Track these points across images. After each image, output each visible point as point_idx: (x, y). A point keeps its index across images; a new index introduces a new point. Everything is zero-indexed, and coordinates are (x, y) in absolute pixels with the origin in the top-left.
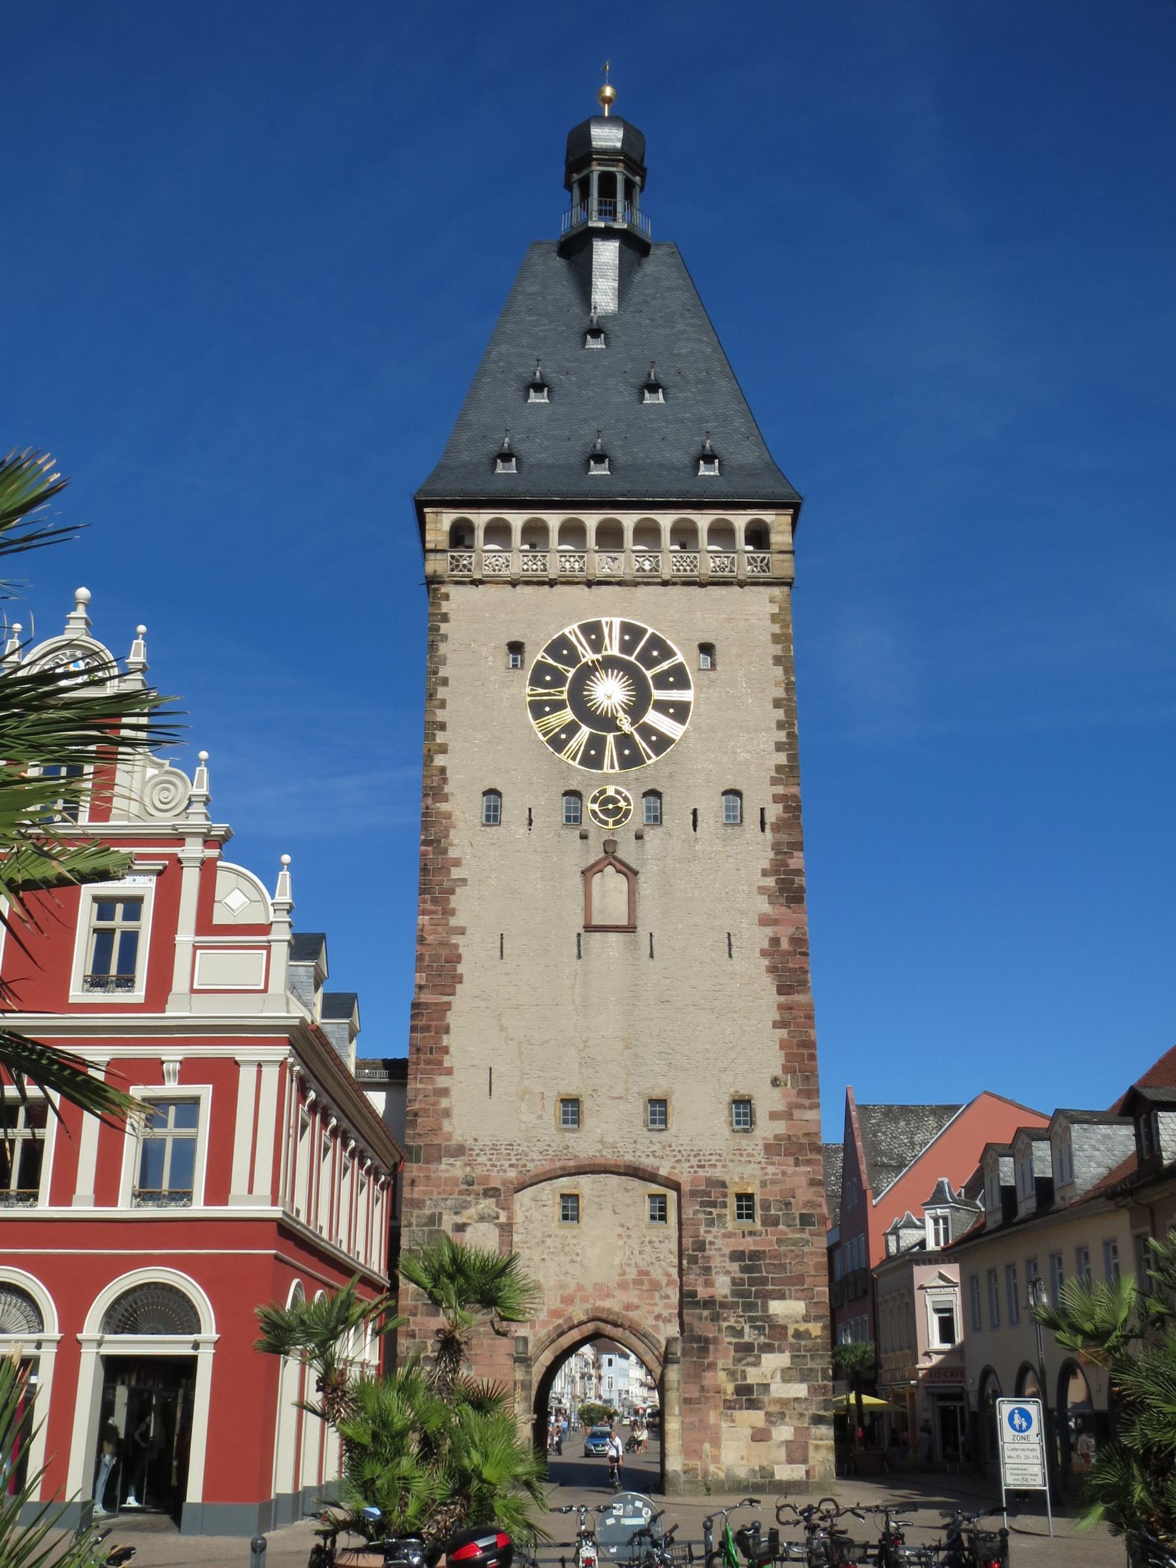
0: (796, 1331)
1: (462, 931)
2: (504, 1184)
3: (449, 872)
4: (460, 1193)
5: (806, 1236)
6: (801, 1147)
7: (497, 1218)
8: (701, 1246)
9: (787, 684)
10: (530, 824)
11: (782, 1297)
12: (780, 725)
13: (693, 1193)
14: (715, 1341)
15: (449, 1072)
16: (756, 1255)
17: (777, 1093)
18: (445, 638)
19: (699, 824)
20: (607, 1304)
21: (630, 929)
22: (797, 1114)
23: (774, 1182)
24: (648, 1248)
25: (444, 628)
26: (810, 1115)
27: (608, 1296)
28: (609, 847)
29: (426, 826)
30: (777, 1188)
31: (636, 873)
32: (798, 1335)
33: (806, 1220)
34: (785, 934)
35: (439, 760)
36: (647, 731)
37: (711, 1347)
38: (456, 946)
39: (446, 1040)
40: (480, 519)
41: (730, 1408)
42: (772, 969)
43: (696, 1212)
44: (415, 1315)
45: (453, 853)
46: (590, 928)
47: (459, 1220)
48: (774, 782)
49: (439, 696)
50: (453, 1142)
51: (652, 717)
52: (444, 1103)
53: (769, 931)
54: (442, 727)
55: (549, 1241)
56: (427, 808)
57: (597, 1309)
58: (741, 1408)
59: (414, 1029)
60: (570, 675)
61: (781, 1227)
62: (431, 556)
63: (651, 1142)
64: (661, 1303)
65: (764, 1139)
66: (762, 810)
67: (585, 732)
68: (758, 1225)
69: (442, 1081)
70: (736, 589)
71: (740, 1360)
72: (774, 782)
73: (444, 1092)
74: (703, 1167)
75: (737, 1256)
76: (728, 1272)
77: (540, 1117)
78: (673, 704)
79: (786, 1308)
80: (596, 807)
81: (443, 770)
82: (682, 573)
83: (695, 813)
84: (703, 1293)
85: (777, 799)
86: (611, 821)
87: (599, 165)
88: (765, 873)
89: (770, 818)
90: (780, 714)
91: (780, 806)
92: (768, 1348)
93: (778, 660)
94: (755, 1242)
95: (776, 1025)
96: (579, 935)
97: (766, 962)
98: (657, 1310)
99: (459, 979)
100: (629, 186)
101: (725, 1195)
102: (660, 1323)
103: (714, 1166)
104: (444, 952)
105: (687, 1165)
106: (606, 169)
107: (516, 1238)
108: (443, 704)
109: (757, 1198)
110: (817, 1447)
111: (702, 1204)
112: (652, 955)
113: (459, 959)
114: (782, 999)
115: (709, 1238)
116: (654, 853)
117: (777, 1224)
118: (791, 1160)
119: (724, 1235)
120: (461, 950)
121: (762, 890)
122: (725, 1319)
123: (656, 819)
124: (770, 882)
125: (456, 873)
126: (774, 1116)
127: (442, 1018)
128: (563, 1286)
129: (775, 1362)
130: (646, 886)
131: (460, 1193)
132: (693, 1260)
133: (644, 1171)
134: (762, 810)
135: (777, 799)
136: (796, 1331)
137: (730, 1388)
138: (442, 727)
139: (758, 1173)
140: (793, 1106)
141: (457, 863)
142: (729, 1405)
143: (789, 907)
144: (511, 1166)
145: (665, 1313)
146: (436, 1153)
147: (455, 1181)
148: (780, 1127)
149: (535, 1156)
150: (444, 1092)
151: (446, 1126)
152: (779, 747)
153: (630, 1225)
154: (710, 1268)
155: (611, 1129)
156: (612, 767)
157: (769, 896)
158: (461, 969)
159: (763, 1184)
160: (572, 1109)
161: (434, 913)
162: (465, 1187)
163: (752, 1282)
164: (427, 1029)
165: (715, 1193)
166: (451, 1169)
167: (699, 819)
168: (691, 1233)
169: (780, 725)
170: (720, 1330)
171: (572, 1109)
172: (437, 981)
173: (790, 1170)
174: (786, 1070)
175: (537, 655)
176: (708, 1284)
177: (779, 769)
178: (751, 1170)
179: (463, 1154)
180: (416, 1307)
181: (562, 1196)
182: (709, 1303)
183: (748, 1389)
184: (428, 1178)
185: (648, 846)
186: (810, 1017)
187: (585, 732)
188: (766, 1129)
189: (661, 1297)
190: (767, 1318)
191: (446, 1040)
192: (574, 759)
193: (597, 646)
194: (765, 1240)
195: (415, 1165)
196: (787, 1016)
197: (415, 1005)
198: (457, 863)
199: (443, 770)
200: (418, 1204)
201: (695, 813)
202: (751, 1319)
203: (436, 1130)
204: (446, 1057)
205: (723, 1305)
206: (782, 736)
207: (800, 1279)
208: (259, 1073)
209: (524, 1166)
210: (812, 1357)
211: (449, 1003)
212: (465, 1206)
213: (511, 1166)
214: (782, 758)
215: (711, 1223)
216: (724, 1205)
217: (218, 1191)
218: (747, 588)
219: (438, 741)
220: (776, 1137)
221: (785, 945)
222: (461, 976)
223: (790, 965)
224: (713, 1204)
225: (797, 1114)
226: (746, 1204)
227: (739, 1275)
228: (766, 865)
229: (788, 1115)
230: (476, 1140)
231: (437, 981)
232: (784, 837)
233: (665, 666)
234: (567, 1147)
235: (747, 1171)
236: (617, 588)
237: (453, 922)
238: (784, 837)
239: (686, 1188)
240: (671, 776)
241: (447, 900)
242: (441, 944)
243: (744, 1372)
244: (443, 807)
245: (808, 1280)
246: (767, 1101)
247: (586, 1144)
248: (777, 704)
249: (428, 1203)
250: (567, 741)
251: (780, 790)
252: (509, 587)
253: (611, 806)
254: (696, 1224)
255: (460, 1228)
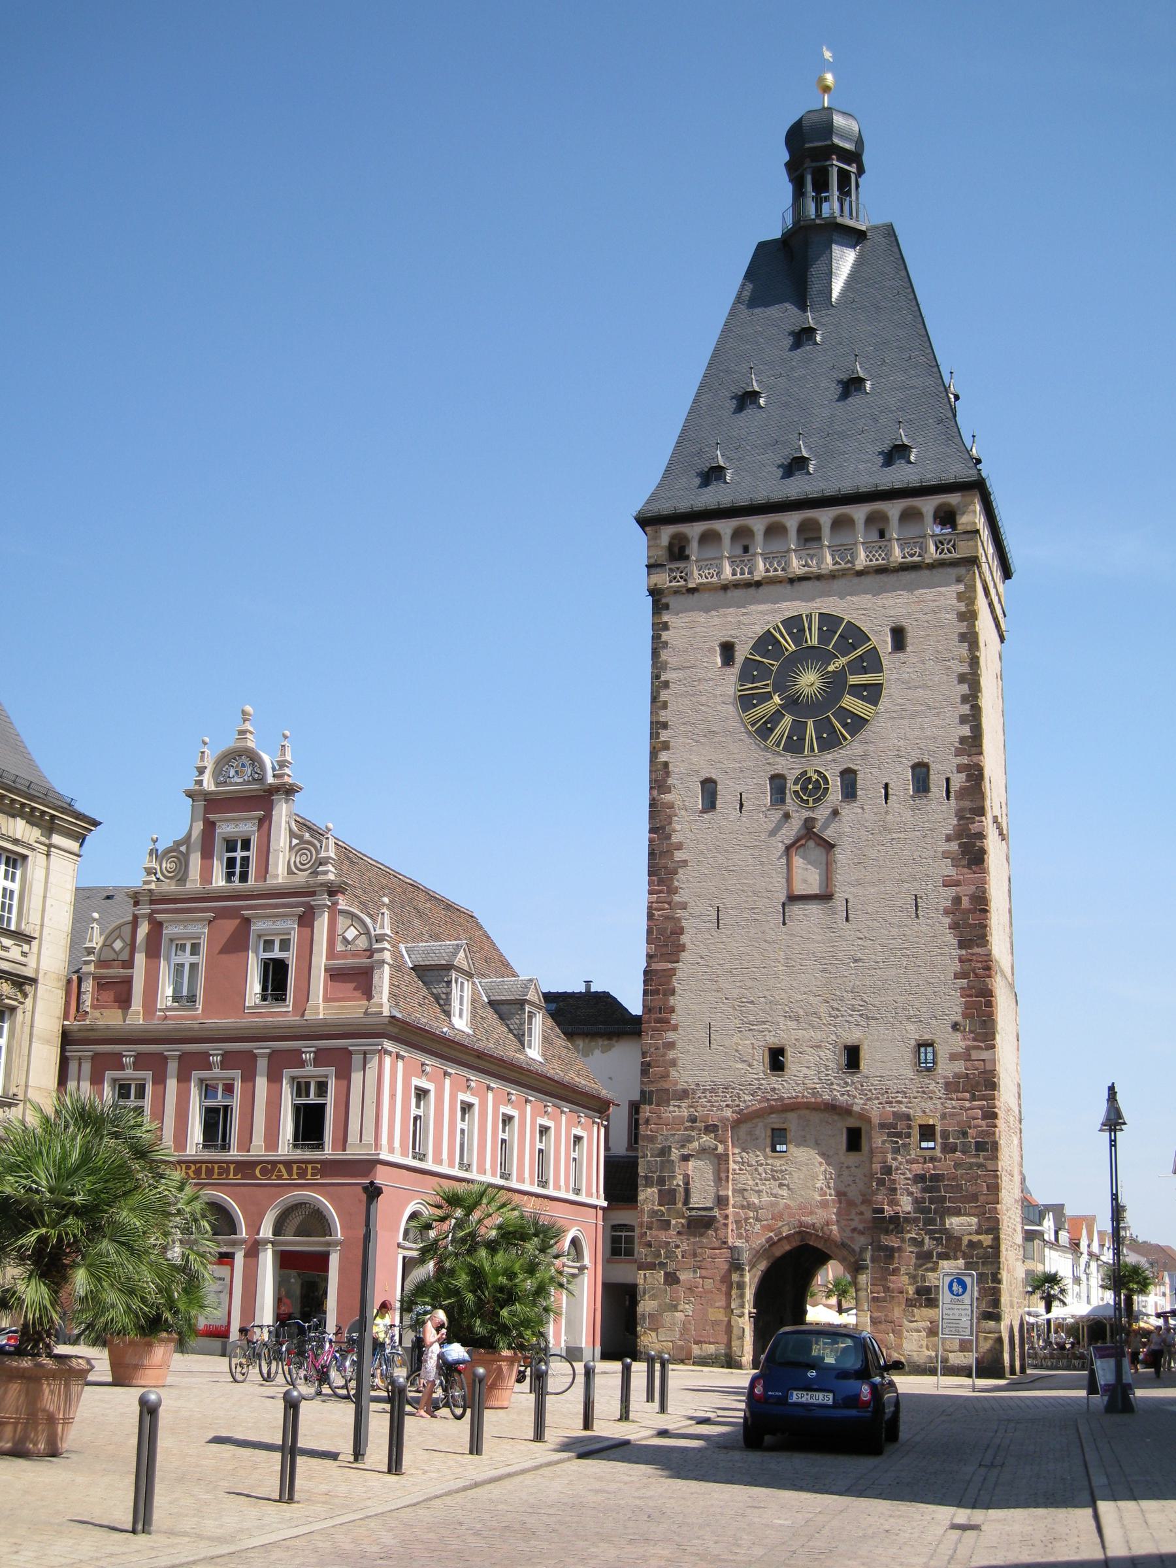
0: (970, 1241)
1: (684, 906)
2: (721, 1121)
3: (673, 854)
4: (686, 1129)
5: (981, 1160)
6: (978, 1083)
7: (716, 1149)
8: (888, 1170)
9: (972, 659)
10: (741, 805)
11: (958, 1213)
12: (965, 699)
13: (882, 1126)
14: (900, 1249)
15: (675, 1028)
16: (936, 1178)
17: (959, 1036)
18: (666, 644)
19: (890, 797)
20: (808, 1220)
21: (825, 897)
22: (975, 1054)
23: (952, 1115)
24: (846, 1173)
25: (665, 636)
26: (985, 1055)
27: (811, 1213)
28: (809, 824)
29: (653, 815)
30: (958, 1118)
31: (833, 846)
32: (971, 1244)
33: (980, 1147)
34: (966, 891)
35: (663, 757)
36: (844, 713)
37: (896, 1255)
38: (679, 919)
39: (672, 1001)
40: (694, 530)
41: (911, 1306)
42: (954, 926)
43: (884, 1142)
44: (650, 1228)
45: (675, 838)
46: (793, 899)
47: (685, 1152)
48: (958, 753)
49: (662, 698)
50: (679, 1087)
51: (849, 702)
52: (671, 1054)
53: (952, 891)
54: (665, 726)
55: (760, 1169)
56: (654, 799)
57: (801, 1224)
58: (921, 1306)
59: (645, 993)
60: (774, 669)
61: (958, 1154)
62: (653, 570)
63: (846, 1083)
64: (857, 1218)
65: (945, 1078)
66: (948, 780)
67: (788, 720)
68: (939, 1155)
69: (670, 1036)
70: (927, 572)
71: (921, 1266)
72: (958, 753)
73: (671, 1045)
74: (891, 1103)
75: (919, 1178)
76: (910, 1194)
77: (750, 1066)
78: (865, 687)
79: (961, 1224)
80: (798, 788)
81: (666, 764)
82: (874, 562)
83: (886, 786)
84: (889, 1211)
85: (960, 768)
86: (811, 799)
87: (812, 161)
88: (948, 839)
89: (955, 786)
90: (964, 688)
91: (963, 776)
92: (945, 1256)
93: (963, 637)
94: (935, 1168)
95: (957, 976)
96: (784, 905)
97: (947, 921)
98: (854, 1224)
99: (682, 948)
100: (844, 177)
101: (910, 1127)
102: (855, 1235)
103: (900, 1102)
104: (669, 926)
105: (876, 1102)
106: (818, 164)
107: (732, 1166)
108: (665, 706)
109: (938, 1129)
110: (986, 1338)
111: (889, 1135)
112: (847, 920)
113: (681, 931)
114: (964, 952)
115: (894, 1164)
116: (850, 826)
117: (953, 1149)
118: (967, 1095)
119: (909, 1162)
120: (684, 923)
121: (946, 855)
122: (909, 1232)
123: (850, 792)
124: (954, 846)
125: (679, 855)
126: (953, 1057)
127: (669, 982)
128: (773, 1205)
129: (950, 1266)
130: (842, 856)
131: (686, 1129)
132: (881, 1182)
133: (841, 1107)
134: (948, 780)
135: (960, 768)
136: (970, 1241)
137: (911, 1290)
138: (665, 726)
139: (939, 1106)
140: (968, 1048)
141: (679, 846)
142: (910, 1303)
143: (970, 869)
144: (727, 1106)
145: (861, 1227)
146: (664, 1097)
147: (681, 1121)
148: (959, 1067)
149: (747, 1098)
150: (671, 1045)
151: (673, 1072)
152: (963, 720)
153: (831, 1153)
154: (895, 1189)
155: (811, 1073)
156: (812, 750)
157: (952, 859)
158: (685, 939)
159: (944, 1116)
160: (776, 1059)
161: (661, 892)
162: (689, 1124)
163: (931, 1202)
164: (656, 992)
165: (901, 1126)
166: (678, 1111)
167: (890, 791)
168: (880, 1159)
169: (965, 699)
170: (903, 1240)
171: (776, 1059)
172: (664, 950)
173: (967, 1104)
174: (965, 1016)
175: (742, 653)
176: (893, 1203)
177: (963, 740)
178: (929, 1105)
179: (687, 1098)
180: (652, 1222)
181: (773, 1129)
182: (895, 1219)
183: (928, 1290)
184: (660, 1118)
185: (844, 820)
186: (988, 968)
187: (788, 720)
188: (947, 1069)
189: (857, 1214)
190: (945, 1231)
191: (672, 1001)
192: (778, 746)
193: (798, 637)
194: (946, 1165)
195: (648, 1107)
196: (967, 966)
197: (646, 973)
198: (679, 846)
199: (666, 764)
200: (652, 1139)
201: (886, 786)
202: (930, 1233)
203: (666, 1076)
204: (674, 1016)
205: (907, 1220)
206: (966, 709)
207: (974, 1197)
208: (365, 1058)
209: (738, 1106)
210: (983, 1263)
211: (674, 969)
212: (690, 1140)
213: (727, 1106)
214: (966, 731)
215: (896, 1151)
216: (909, 1136)
217: (342, 1141)
218: (935, 571)
219: (662, 739)
220: (957, 1076)
221: (965, 903)
222: (684, 945)
223: (971, 921)
224: (899, 1135)
225: (975, 1054)
226: (927, 1132)
227: (919, 1195)
228: (949, 830)
229: (966, 1056)
230: (698, 1085)
231: (664, 950)
232: (967, 804)
233: (859, 652)
234: (773, 1090)
235: (929, 1107)
236: (817, 583)
237: (676, 898)
238: (967, 804)
239: (876, 1121)
240: (865, 755)
241: (672, 879)
242: (667, 918)
243: (923, 1276)
244: (667, 797)
245: (982, 1198)
246: (950, 1043)
247: (788, 1087)
248: (962, 679)
249: (660, 1137)
250: (771, 730)
251: (964, 760)
252: (721, 593)
253: (810, 786)
254: (885, 1152)
255: (685, 1158)
